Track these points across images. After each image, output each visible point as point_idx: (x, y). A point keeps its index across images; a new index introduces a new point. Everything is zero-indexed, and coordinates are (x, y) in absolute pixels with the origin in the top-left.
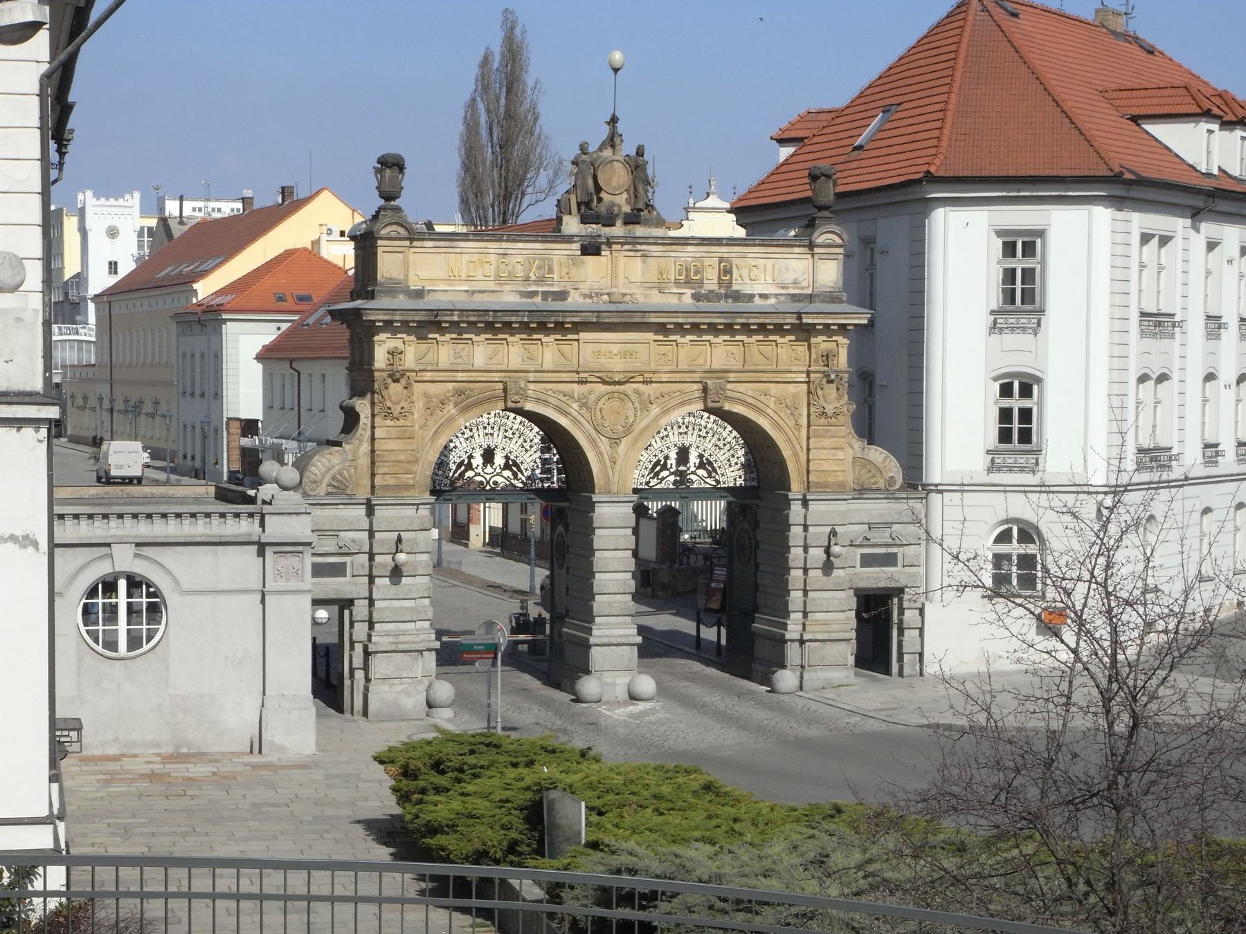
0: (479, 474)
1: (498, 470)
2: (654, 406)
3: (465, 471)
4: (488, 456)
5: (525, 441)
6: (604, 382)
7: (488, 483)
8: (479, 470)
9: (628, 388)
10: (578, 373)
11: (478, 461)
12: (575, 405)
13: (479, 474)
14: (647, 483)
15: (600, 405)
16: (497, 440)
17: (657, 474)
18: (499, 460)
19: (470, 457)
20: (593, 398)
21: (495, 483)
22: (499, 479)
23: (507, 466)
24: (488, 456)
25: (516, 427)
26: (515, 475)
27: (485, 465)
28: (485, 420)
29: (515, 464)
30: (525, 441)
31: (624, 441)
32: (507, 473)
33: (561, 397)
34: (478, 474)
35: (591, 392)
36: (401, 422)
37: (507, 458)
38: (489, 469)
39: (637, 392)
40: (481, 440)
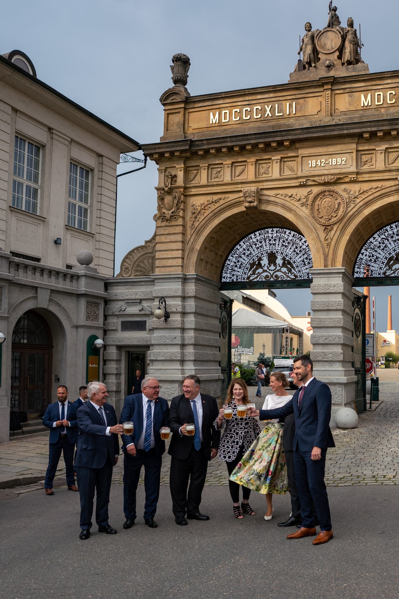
0: (266, 271)
1: (278, 268)
2: (358, 201)
3: (257, 269)
4: (272, 258)
5: (297, 248)
6: (320, 184)
7: (272, 276)
8: (266, 268)
9: (339, 189)
10: (297, 178)
11: (265, 261)
12: (297, 204)
13: (266, 271)
14: (384, 273)
15: (317, 202)
16: (278, 248)
17: (390, 268)
18: (279, 261)
19: (260, 259)
20: (311, 197)
21: (276, 276)
22: (279, 274)
23: (284, 265)
24: (272, 258)
25: (290, 238)
26: (290, 271)
27: (270, 264)
28: (270, 235)
29: (289, 263)
30: (297, 248)
31: (335, 227)
32: (284, 269)
33: (287, 198)
34: (264, 271)
35: (310, 193)
36: (173, 223)
37: (284, 259)
38: (272, 267)
39: (345, 190)
40: (267, 248)
